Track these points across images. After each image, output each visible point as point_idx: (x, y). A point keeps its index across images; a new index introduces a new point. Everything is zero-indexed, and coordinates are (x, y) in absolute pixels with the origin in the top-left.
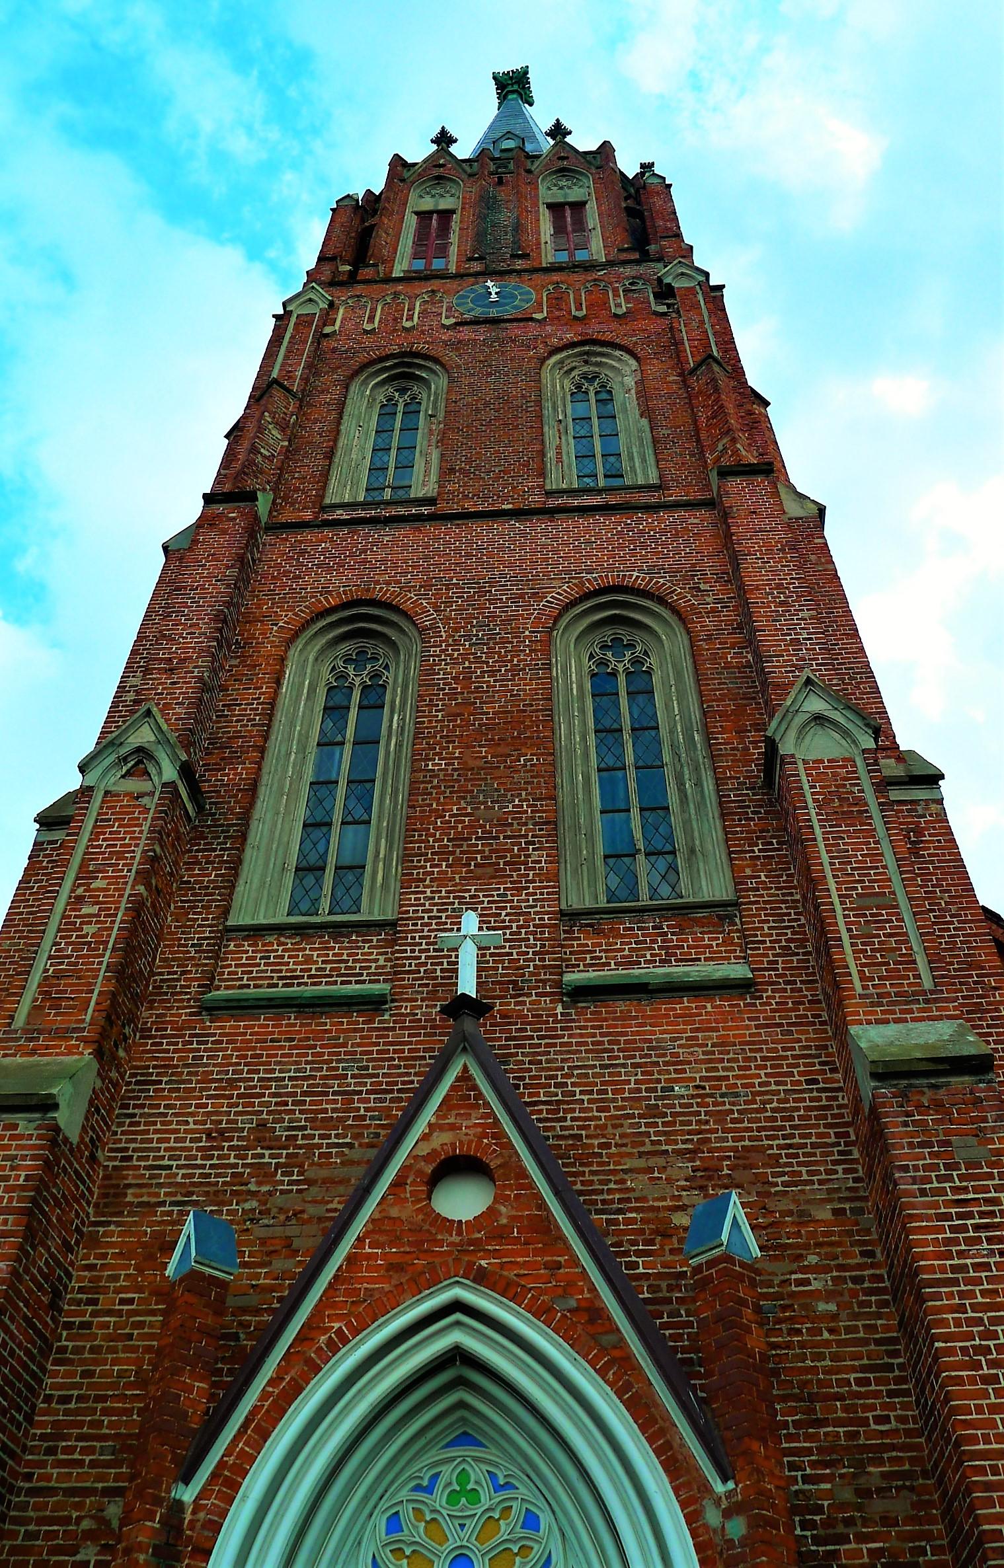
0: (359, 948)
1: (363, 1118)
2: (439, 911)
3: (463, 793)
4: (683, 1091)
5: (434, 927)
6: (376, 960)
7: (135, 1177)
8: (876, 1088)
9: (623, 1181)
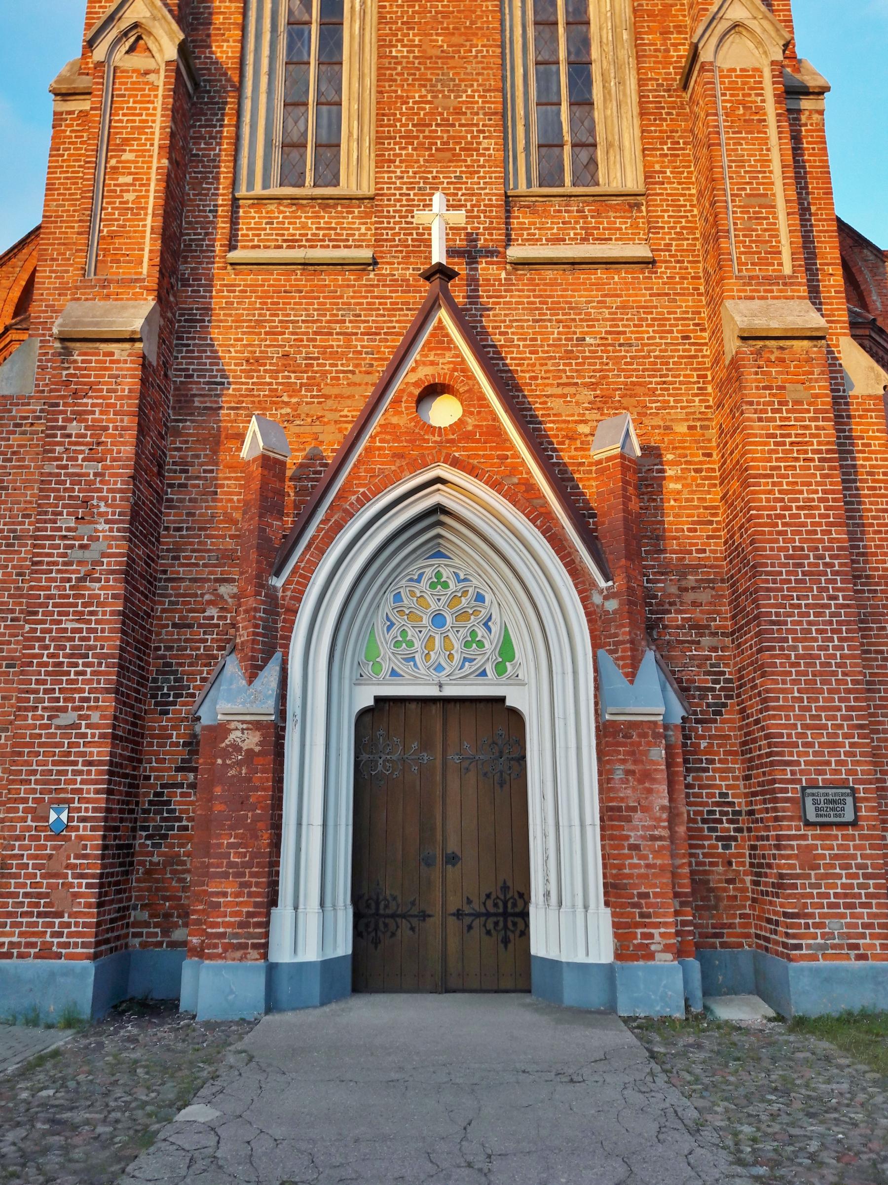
0: (344, 218)
1: (360, 353)
2: (408, 189)
3: (424, 82)
4: (592, 341)
5: (404, 203)
6: (359, 229)
7: (198, 389)
8: (739, 347)
9: (545, 403)
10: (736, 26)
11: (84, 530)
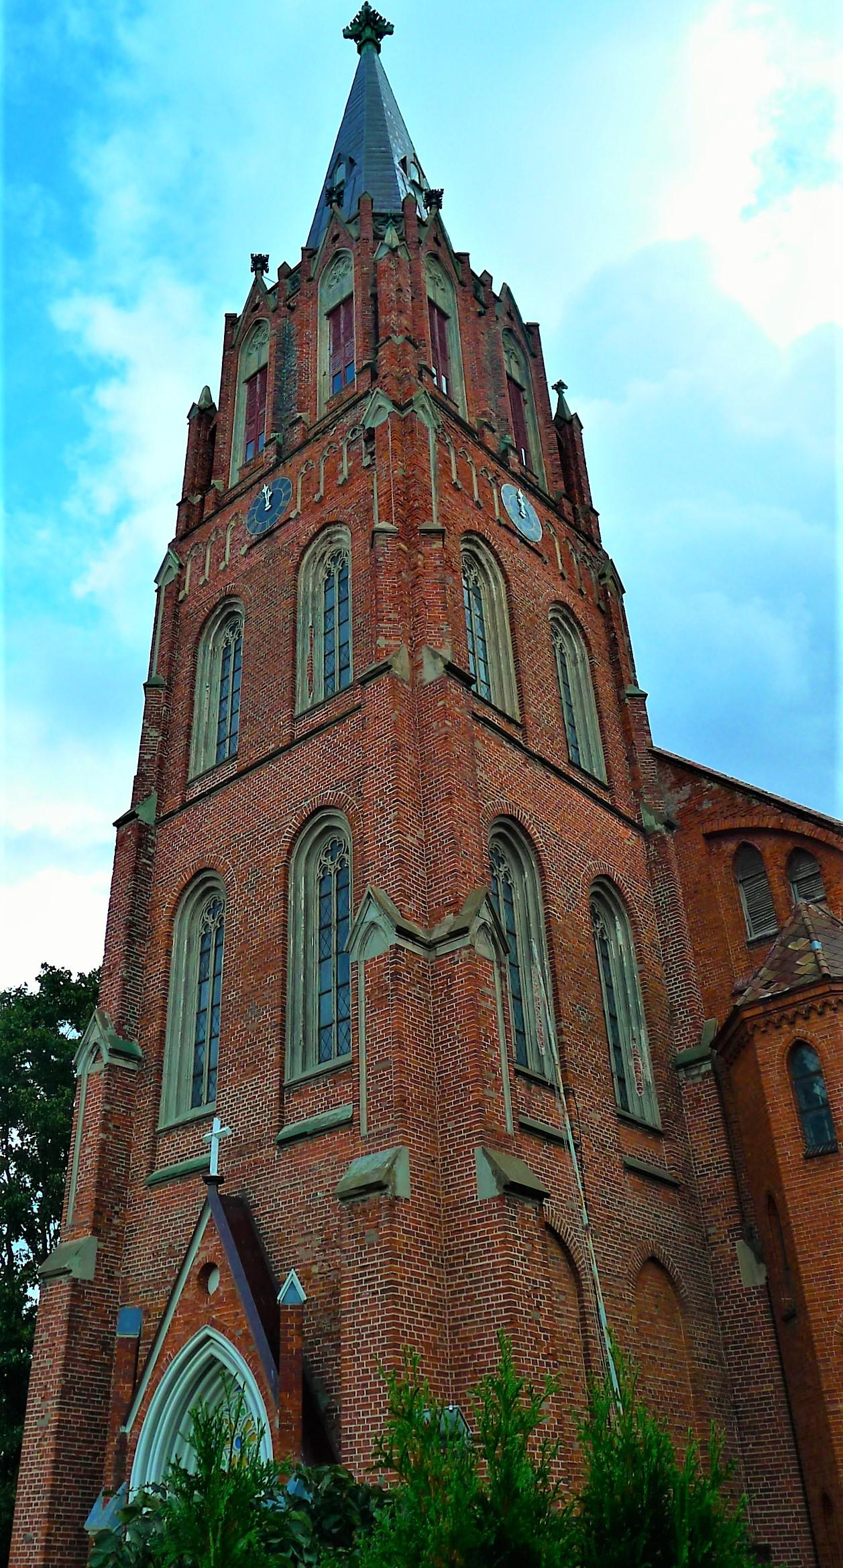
10: (373, 924)
11: (44, 1403)
